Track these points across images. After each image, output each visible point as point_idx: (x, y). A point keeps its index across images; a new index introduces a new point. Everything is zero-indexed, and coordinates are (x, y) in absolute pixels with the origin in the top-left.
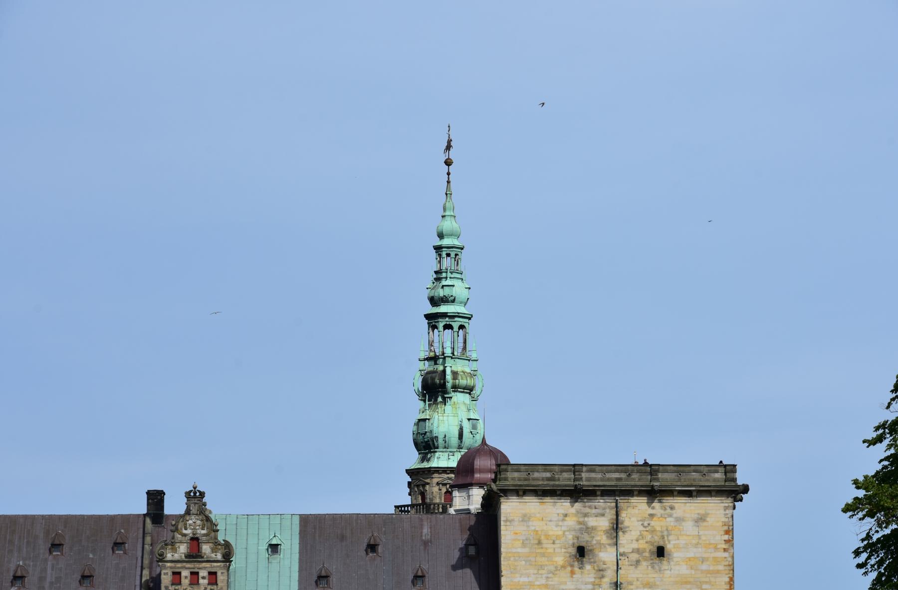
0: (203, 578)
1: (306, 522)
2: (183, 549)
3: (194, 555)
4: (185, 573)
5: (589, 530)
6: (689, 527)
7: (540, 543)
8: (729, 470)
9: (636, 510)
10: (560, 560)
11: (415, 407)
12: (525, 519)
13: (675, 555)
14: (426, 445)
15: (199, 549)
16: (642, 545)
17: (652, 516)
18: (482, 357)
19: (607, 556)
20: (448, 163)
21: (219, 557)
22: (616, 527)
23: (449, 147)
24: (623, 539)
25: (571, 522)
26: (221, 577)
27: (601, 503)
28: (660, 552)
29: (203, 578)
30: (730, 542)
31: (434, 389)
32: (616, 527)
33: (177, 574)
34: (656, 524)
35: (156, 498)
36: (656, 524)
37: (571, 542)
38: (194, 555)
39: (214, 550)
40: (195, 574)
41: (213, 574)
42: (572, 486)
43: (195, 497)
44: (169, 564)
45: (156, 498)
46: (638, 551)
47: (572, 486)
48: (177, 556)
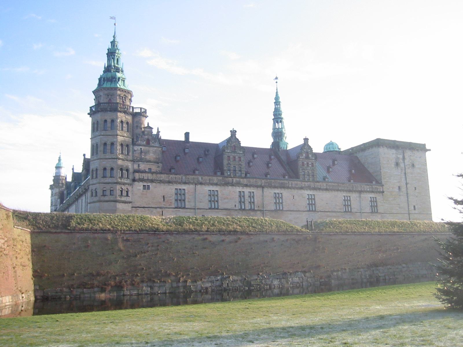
0: (310, 164)
2: (304, 155)
3: (307, 157)
4: (305, 163)
5: (398, 158)
7: (388, 161)
8: (424, 145)
9: (408, 153)
10: (393, 166)
13: (417, 166)
15: (308, 156)
17: (411, 155)
19: (402, 165)
20: (277, 82)
21: (314, 159)
23: (276, 78)
24: (406, 161)
25: (394, 156)
26: (314, 165)
27: (400, 151)
28: (413, 165)
29: (310, 164)
32: (404, 158)
33: (303, 163)
34: (412, 158)
36: (412, 158)
37: (395, 161)
38: (307, 157)
39: (312, 156)
40: (308, 163)
41: (312, 164)
44: (301, 160)
46: (409, 165)
48: (303, 157)
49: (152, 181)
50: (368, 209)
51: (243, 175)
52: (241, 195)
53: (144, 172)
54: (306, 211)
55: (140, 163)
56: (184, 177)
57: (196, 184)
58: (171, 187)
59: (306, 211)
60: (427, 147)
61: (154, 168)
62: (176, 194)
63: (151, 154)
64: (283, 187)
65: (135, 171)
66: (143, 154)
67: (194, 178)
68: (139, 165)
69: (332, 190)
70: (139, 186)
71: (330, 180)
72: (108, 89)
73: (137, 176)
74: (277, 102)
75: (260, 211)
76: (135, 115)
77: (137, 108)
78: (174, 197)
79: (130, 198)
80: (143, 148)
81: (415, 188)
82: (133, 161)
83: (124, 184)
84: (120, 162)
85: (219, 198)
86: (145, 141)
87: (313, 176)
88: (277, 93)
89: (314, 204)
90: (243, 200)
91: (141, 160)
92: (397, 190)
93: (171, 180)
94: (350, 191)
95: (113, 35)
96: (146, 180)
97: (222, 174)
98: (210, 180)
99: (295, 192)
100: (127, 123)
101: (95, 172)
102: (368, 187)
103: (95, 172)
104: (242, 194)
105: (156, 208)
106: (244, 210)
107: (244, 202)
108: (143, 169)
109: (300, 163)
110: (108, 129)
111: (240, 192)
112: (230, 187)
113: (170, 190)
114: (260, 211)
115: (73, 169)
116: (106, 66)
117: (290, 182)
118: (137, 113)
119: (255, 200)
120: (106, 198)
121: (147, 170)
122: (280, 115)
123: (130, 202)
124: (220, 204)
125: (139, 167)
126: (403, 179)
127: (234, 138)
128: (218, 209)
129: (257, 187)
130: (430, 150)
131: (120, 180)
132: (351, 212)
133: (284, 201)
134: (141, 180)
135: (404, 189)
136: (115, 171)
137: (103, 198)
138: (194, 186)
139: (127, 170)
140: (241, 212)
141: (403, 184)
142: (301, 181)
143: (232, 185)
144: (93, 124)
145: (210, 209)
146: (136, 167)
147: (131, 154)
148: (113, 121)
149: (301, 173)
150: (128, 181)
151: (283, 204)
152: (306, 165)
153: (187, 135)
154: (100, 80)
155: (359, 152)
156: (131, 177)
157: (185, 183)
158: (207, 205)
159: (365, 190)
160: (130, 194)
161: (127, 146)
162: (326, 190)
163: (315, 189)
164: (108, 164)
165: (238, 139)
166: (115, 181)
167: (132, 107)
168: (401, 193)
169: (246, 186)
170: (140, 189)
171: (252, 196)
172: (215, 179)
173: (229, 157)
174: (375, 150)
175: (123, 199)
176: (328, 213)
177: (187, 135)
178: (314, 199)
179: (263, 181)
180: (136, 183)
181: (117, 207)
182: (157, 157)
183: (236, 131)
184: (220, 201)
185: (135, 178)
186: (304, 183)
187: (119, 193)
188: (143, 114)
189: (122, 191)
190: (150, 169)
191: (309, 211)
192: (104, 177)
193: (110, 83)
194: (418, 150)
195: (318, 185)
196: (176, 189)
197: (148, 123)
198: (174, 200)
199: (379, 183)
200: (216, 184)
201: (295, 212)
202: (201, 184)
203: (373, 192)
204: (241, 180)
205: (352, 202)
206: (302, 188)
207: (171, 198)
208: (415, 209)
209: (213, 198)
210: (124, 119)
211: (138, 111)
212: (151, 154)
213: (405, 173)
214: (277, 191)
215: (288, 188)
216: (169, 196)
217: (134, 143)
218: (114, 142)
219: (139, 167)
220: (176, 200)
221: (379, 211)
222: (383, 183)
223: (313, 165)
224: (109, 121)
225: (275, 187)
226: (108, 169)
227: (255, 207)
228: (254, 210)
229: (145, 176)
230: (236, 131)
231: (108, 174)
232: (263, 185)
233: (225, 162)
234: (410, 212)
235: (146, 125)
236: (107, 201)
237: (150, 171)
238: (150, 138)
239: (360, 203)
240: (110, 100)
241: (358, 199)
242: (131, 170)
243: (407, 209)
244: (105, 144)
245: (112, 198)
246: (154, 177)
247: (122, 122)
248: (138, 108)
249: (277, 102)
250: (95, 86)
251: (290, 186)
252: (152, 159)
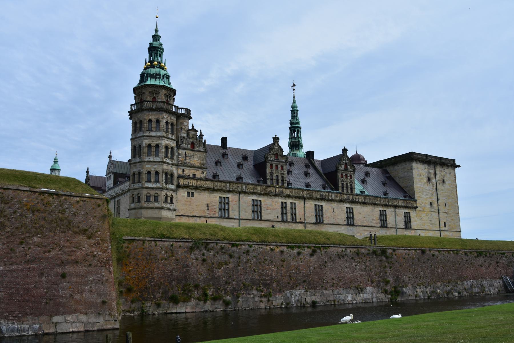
2: (343, 166)
3: (346, 169)
4: (344, 174)
5: (430, 173)
6: (448, 174)
8: (454, 161)
9: (438, 169)
10: (425, 181)
16: (440, 179)
19: (434, 181)
23: (294, 85)
24: (437, 176)
25: (426, 170)
26: (353, 177)
27: (432, 167)
28: (444, 181)
30: (455, 180)
32: (435, 174)
33: (342, 175)
34: (442, 173)
38: (346, 169)
39: (351, 168)
40: (346, 175)
46: (439, 180)
49: (197, 188)
50: (402, 225)
51: (286, 185)
52: (283, 206)
53: (188, 177)
54: (345, 225)
55: (184, 168)
56: (228, 185)
57: (240, 193)
58: (216, 195)
59: (345, 225)
60: (457, 163)
61: (198, 175)
62: (220, 203)
63: (196, 159)
64: (323, 199)
65: (179, 177)
66: (187, 158)
67: (238, 187)
68: (183, 170)
69: (369, 204)
70: (183, 194)
71: (367, 193)
72: (153, 86)
73: (182, 182)
74: (294, 112)
75: (302, 223)
76: (179, 116)
77: (181, 108)
78: (217, 206)
79: (174, 205)
80: (187, 152)
81: (446, 204)
82: (177, 165)
83: (171, 190)
84: (165, 167)
85: (263, 209)
86: (189, 144)
87: (351, 188)
88: (294, 101)
89: (353, 218)
90: (285, 212)
91: (186, 165)
92: (428, 206)
93: (215, 188)
94: (386, 206)
95: (155, 28)
96: (190, 186)
97: (265, 182)
98: (253, 188)
99: (334, 205)
100: (172, 124)
101: (137, 176)
102: (402, 202)
103: (137, 176)
104: (284, 205)
105: (200, 217)
106: (287, 221)
107: (286, 214)
108: (187, 175)
109: (340, 176)
110: (153, 129)
111: (282, 203)
112: (273, 197)
113: (215, 198)
114: (302, 223)
115: (87, 172)
116: (148, 61)
117: (330, 194)
118: (182, 114)
119: (297, 212)
120: (151, 205)
121: (191, 176)
122: (298, 123)
123: (174, 210)
124: (263, 215)
125: (183, 172)
126: (435, 195)
127: (277, 144)
128: (261, 220)
129: (299, 198)
130: (459, 166)
131: (165, 186)
132: (386, 227)
133: (324, 214)
134: (185, 187)
135: (435, 205)
136: (160, 176)
137: (145, 205)
138: (238, 195)
139: (172, 175)
140: (283, 224)
141: (434, 200)
142: (339, 193)
143: (276, 195)
144: (134, 124)
145: (253, 220)
146: (180, 172)
147: (175, 157)
148: (158, 121)
149: (340, 185)
150: (173, 187)
151: (324, 216)
152: (344, 177)
153: (224, 140)
154: (142, 75)
155: (389, 166)
156: (175, 183)
157: (230, 191)
158: (250, 216)
159: (400, 204)
160: (174, 201)
161: (172, 148)
162: (364, 203)
163: (353, 202)
164: (152, 168)
165: (280, 147)
166: (161, 187)
167: (177, 107)
168: (433, 210)
169: (289, 196)
170: (184, 196)
171: (294, 207)
172: (259, 189)
173: (271, 166)
174: (407, 165)
175: (168, 206)
176: (366, 228)
177: (224, 140)
178: (353, 213)
179: (305, 192)
180: (180, 189)
181: (162, 214)
182: (202, 162)
183: (278, 139)
184: (263, 211)
185: (179, 183)
186: (343, 196)
187: (163, 198)
188: (187, 115)
189: (166, 198)
190: (194, 175)
191: (348, 225)
192: (149, 181)
193: (154, 79)
194: (448, 166)
195: (356, 198)
196: (220, 197)
197: (193, 125)
198: (218, 209)
199: (412, 198)
200: (260, 194)
201: (334, 226)
202: (245, 193)
203: (407, 207)
204: (284, 190)
205: (388, 216)
206: (341, 201)
207: (215, 207)
208: (445, 226)
209: (257, 209)
210: (169, 121)
211: (183, 111)
212: (196, 159)
213: (436, 189)
214: (318, 203)
215: (329, 200)
216: (213, 204)
217: (179, 147)
218: (160, 144)
219: (183, 172)
220: (220, 209)
221: (412, 227)
222: (416, 198)
223: (351, 176)
224: (154, 120)
225: (316, 199)
226: (153, 173)
227: (297, 218)
228: (296, 222)
229: (190, 182)
230: (278, 139)
231: (153, 179)
232: (305, 196)
233: (268, 170)
234: (441, 229)
235: (190, 128)
236: (152, 208)
237: (194, 177)
238: (195, 141)
239: (395, 218)
240: (154, 98)
241: (393, 214)
242: (176, 175)
243: (438, 226)
244: (149, 146)
245: (156, 204)
247: (167, 123)
248: (183, 108)
249: (294, 112)
250: (136, 82)
251: (330, 198)
252: (197, 165)
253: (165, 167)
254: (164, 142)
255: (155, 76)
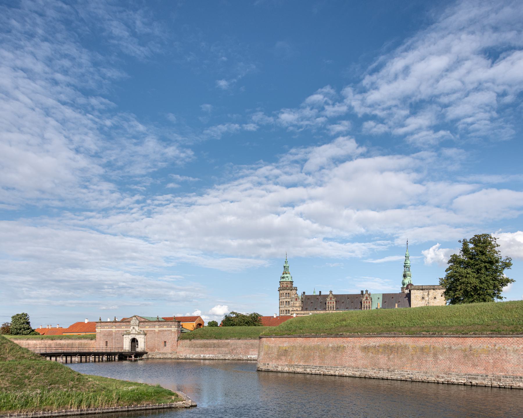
1: (383, 294)
3: (367, 299)
9: (432, 291)
11: (402, 278)
12: (415, 293)
14: (404, 284)
18: (412, 272)
19: (427, 298)
22: (428, 294)
28: (435, 298)
31: (405, 276)
32: (428, 294)
35: (362, 292)
38: (367, 299)
42: (422, 288)
43: (367, 291)
45: (362, 292)
47: (422, 288)
84: (286, 308)
91: (294, 306)
149: (363, 306)
153: (320, 292)
177: (320, 292)
246: (299, 312)
253: (286, 308)
254: (285, 300)
255: (283, 278)
